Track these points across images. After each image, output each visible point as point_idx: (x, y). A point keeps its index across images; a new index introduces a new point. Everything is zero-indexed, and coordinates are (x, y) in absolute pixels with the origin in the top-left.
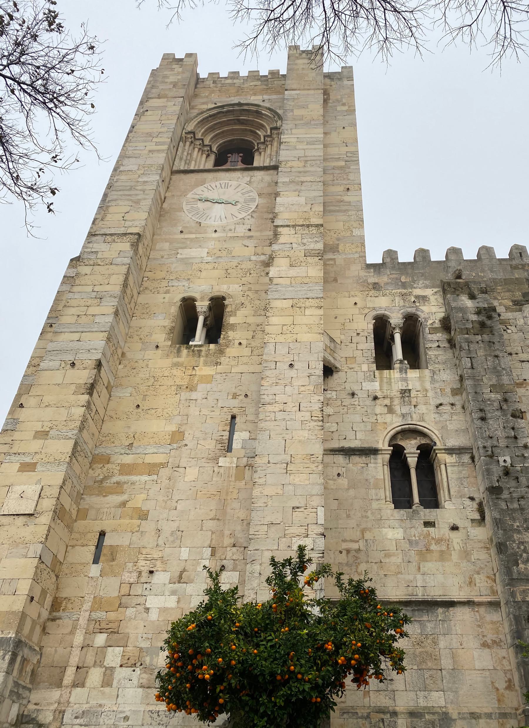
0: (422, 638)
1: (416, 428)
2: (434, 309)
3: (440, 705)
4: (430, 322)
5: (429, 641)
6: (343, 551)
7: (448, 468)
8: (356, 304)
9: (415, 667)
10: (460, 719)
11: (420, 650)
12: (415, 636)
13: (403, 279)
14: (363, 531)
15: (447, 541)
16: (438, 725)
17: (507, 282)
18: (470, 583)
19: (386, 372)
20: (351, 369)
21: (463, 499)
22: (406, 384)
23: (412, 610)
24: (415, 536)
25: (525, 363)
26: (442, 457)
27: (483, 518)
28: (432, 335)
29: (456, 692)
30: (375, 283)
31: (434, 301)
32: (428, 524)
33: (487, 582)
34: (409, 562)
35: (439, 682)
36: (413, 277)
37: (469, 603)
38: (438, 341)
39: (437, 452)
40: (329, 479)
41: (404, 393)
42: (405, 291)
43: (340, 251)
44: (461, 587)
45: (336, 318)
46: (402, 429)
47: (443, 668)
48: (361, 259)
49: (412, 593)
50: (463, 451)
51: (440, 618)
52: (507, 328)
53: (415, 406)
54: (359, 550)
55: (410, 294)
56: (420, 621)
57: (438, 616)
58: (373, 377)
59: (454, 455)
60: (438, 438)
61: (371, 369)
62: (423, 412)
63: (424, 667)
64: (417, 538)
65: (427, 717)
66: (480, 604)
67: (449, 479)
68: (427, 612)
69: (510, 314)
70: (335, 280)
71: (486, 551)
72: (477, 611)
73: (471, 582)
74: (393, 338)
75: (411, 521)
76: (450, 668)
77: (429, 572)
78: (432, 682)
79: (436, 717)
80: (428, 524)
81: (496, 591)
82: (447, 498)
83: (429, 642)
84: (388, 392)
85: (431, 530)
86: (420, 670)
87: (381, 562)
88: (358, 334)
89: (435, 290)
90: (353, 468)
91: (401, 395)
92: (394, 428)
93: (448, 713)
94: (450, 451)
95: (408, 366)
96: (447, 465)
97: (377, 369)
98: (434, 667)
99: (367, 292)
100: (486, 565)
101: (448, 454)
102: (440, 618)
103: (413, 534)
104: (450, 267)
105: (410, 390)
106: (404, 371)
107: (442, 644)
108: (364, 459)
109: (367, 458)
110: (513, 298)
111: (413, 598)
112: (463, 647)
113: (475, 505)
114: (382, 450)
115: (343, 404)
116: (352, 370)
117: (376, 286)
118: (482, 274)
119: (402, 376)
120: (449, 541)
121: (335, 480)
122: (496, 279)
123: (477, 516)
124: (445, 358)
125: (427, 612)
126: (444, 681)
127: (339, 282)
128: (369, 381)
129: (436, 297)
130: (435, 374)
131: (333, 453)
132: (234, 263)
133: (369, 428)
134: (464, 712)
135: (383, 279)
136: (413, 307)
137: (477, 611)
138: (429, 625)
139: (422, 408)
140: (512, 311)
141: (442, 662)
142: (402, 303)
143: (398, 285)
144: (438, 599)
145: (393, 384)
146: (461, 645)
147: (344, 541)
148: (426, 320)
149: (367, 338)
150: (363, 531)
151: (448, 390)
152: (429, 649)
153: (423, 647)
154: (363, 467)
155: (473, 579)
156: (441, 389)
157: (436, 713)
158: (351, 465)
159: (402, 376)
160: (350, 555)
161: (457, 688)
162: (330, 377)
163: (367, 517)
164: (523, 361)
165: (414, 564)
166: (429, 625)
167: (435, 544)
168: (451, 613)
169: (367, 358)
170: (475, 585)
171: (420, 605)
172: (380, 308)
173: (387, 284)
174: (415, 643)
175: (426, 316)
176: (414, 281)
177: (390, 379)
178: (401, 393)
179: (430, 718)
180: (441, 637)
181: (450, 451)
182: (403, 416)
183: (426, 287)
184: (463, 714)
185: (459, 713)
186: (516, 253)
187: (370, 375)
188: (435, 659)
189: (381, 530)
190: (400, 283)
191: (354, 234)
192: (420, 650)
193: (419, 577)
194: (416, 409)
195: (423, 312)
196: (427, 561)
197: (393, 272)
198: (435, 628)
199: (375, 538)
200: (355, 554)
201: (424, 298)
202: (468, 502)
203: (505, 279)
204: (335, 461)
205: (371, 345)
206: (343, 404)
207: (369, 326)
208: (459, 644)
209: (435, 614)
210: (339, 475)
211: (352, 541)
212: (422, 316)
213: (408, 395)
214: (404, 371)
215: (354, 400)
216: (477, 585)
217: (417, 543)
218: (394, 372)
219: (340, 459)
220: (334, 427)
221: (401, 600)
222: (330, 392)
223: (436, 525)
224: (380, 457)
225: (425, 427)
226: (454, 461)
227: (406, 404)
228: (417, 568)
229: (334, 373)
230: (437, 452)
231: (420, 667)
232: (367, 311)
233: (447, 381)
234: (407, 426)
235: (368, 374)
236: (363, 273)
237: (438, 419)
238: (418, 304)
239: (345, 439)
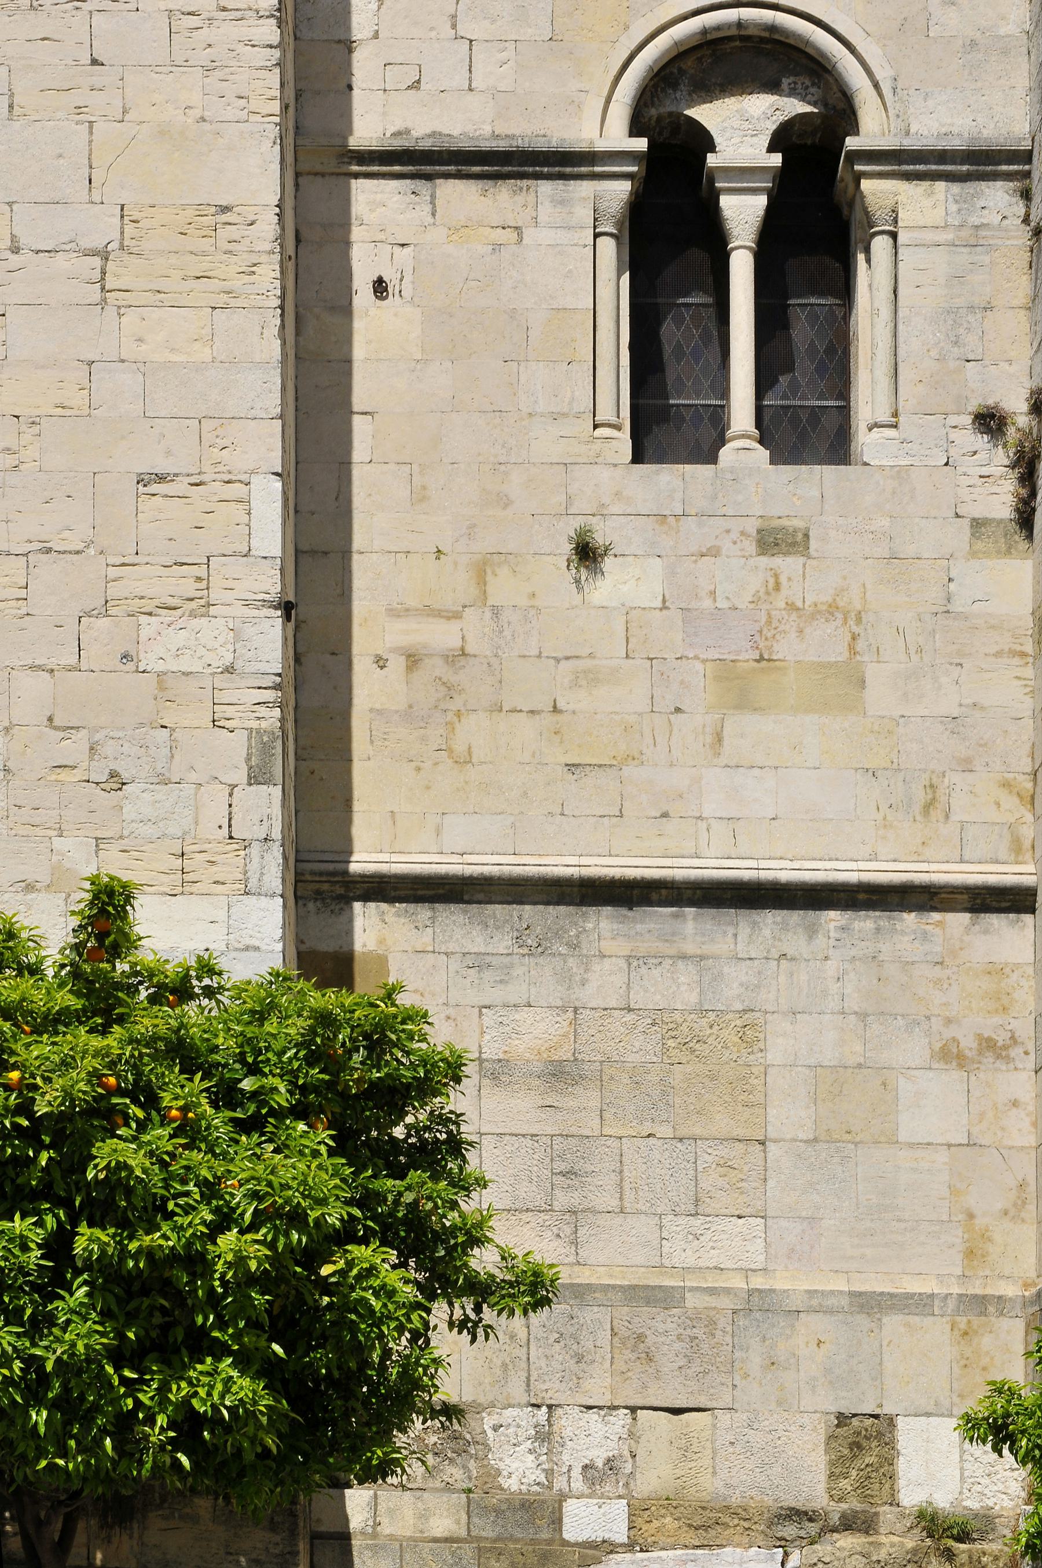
1: (773, 28)
6: (391, 657)
7: (900, 251)
24: (713, 593)
34: (678, 710)
46: (705, 31)
59: (941, 186)
85: (788, 565)
87: (555, 709)
96: (901, 238)
138: (737, 976)
166: (737, 976)
198: (758, 986)
223: (813, 544)
224: (586, 188)
228: (709, 739)
239: (416, 85)
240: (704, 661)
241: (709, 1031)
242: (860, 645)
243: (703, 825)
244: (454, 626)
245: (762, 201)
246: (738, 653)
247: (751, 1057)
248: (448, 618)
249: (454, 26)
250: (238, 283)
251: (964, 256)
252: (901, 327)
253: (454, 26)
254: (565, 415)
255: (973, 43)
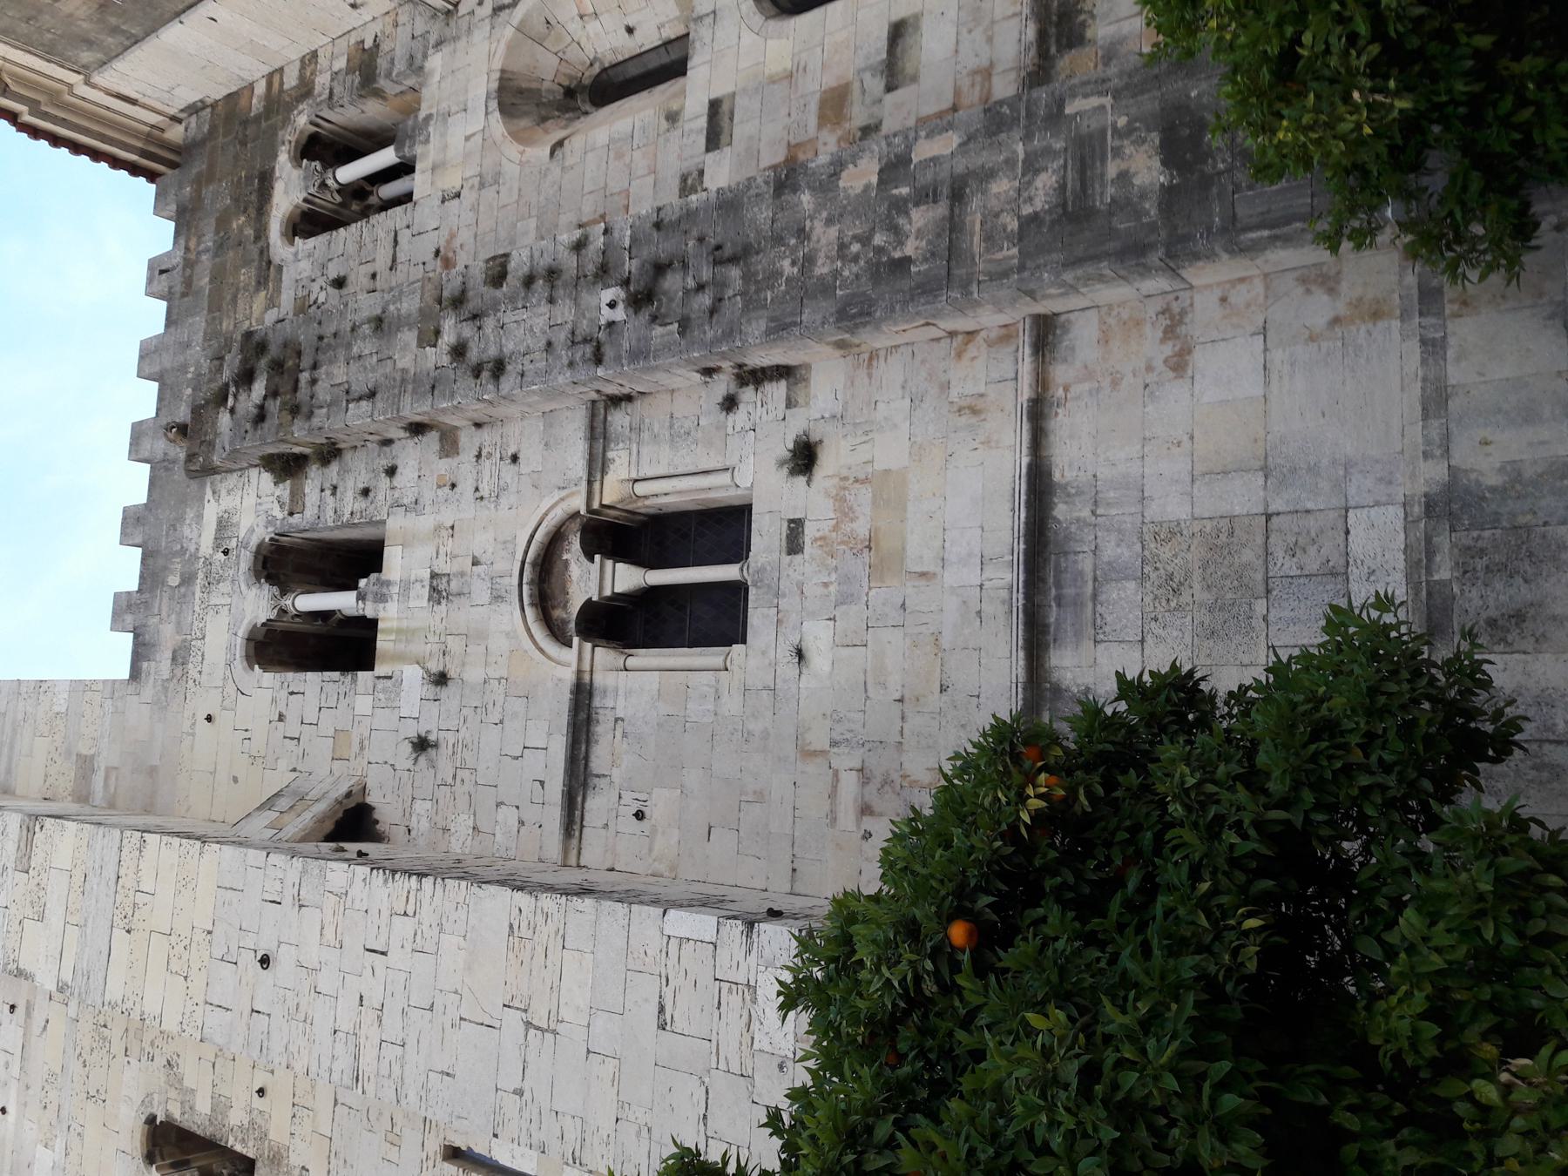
0: (1153, 576)
1: (534, 564)
2: (251, 500)
3: (1399, 524)
4: (278, 513)
5: (1166, 552)
6: (864, 827)
7: (642, 475)
8: (209, 719)
9: (1260, 607)
10: (1447, 451)
11: (1197, 586)
12: (1148, 599)
13: (174, 580)
14: (809, 754)
15: (847, 484)
16: (1475, 534)
17: (215, 307)
18: (974, 411)
19: (383, 643)
20: (362, 748)
21: (730, 430)
22: (418, 585)
23: (1059, 605)
24: (826, 585)
25: (398, 255)
26: (612, 491)
27: (783, 372)
28: (308, 504)
29: (1348, 466)
30: (174, 659)
31: (231, 497)
32: (794, 540)
33: (973, 359)
34: (904, 604)
35: (1312, 523)
36: (175, 554)
37: (1038, 414)
38: (322, 490)
39: (596, 505)
40: (651, 850)
41: (439, 592)
42: (201, 575)
43: (92, 752)
44: (987, 442)
45: (235, 780)
46: (532, 604)
47: (1261, 509)
48: (116, 694)
49: (1003, 602)
50: (599, 430)
51: (1085, 513)
52: (315, 302)
53: (475, 563)
54: (862, 770)
55: (208, 562)
56: (1095, 579)
57: (1078, 520)
58: (388, 683)
59: (610, 455)
60: (562, 499)
61: (370, 685)
62: (491, 540)
63: (1259, 576)
64: (834, 576)
65: (1444, 573)
66: (1041, 382)
67: (672, 472)
68: (1066, 553)
69: (284, 297)
70: (152, 771)
71: (882, 360)
72: (1066, 389)
73: (973, 409)
74: (325, 615)
75: (784, 596)
76: (1261, 481)
77: (939, 543)
78: (1312, 550)
79: (1443, 541)
80: (794, 540)
81: (1003, 331)
82: (724, 479)
83: (1169, 555)
84: (431, 638)
85: (810, 531)
86: (1268, 591)
87: (901, 700)
88: (281, 718)
89: (209, 494)
90: (623, 766)
91: (444, 602)
92: (528, 630)
93: (1426, 495)
94: (597, 465)
95: (373, 576)
96: (634, 475)
97: (371, 668)
98: (1260, 540)
99: (190, 682)
100: (923, 362)
101: (604, 472)
102: (1085, 513)
103: (821, 590)
104: (165, 454)
105: (434, 576)
106: (385, 590)
107: (1171, 506)
108: (602, 730)
109: (601, 718)
110: (251, 289)
111: (1019, 599)
112: (1185, 438)
113: (748, 394)
114: (579, 672)
115: (450, 781)
116: (366, 743)
117: (180, 657)
118: (192, 369)
119: (395, 597)
120: (846, 479)
121: (651, 837)
122: (205, 333)
123: (777, 391)
124: (363, 471)
125: (1066, 553)
126: (1310, 505)
127: (157, 762)
128: (398, 694)
129: (223, 493)
130: (401, 502)
131: (577, 827)
132: (75, 1067)
133: (517, 705)
134: (1420, 440)
135: (167, 636)
136: (238, 557)
137: (1066, 389)
138: (1110, 550)
139: (481, 542)
140: (278, 290)
141: (1238, 510)
142: (225, 587)
143: (184, 596)
144: (1023, 516)
145: (414, 624)
146: (1179, 444)
147: (833, 819)
148: (271, 521)
149: (292, 693)
150: (809, 754)
151: (444, 466)
152: (1196, 554)
153: (1188, 575)
154: (625, 735)
155: (964, 403)
156: (439, 487)
157: (1428, 540)
158: (616, 773)
159: (395, 597)
160: (877, 805)
161: (1334, 462)
162: (376, 816)
163: (766, 735)
164: (394, 260)
165: (910, 591)
166: (1110, 550)
167: (852, 520)
168: (1070, 475)
169: (342, 697)
170: (982, 395)
171: (1044, 580)
172: (229, 648)
173: (179, 623)
174: (1173, 604)
175: (262, 520)
176: (183, 551)
177: (399, 631)
178: (439, 603)
179: (1448, 564)
180: (1153, 511)
181: (597, 465)
182: (497, 598)
183: (199, 517)
184: (1428, 441)
185: (1426, 455)
186: (159, 282)
187: (384, 691)
188: (1231, 534)
189: (804, 694)
190: (183, 590)
191: (63, 710)
192: (1197, 586)
193: (950, 577)
194: (483, 560)
195: (252, 530)
196: (904, 549)
197: (157, 605)
198: (1119, 531)
199: (829, 713)
200: (872, 788)
201: (223, 525)
202: (739, 417)
203: (210, 311)
204: (600, 824)
205: (312, 680)
206: (450, 781)
207: (268, 683)
208: (1175, 450)
209: (1073, 528)
210: (639, 815)
211: (833, 795)
212: (263, 534)
213: (445, 580)
214: (385, 590)
215: (443, 745)
216: (982, 389)
217: (846, 580)
218: (383, 619)
219: (596, 806)
220: (508, 816)
221: (1021, 642)
222: (414, 819)
224: (599, 679)
225: (532, 536)
226: (624, 454)
227: (466, 591)
228: (923, 582)
229: (369, 800)
230: (596, 505)
231: (1261, 589)
232: (231, 689)
233: (420, 469)
234: (525, 588)
235: (381, 696)
236: (148, 690)
237: (513, 499)
238: (233, 544)
239: (542, 783)
240: (870, 588)
241: (1162, 571)
242: (862, 476)
243: (987, 584)
244: (843, 776)
245: (620, 566)
246: (864, 564)
247: (1185, 532)
248: (838, 781)
249: (517, 758)
250: (552, 926)
251: (646, 435)
252: (680, 471)
253: (517, 758)
254: (717, 690)
255: (546, 445)
